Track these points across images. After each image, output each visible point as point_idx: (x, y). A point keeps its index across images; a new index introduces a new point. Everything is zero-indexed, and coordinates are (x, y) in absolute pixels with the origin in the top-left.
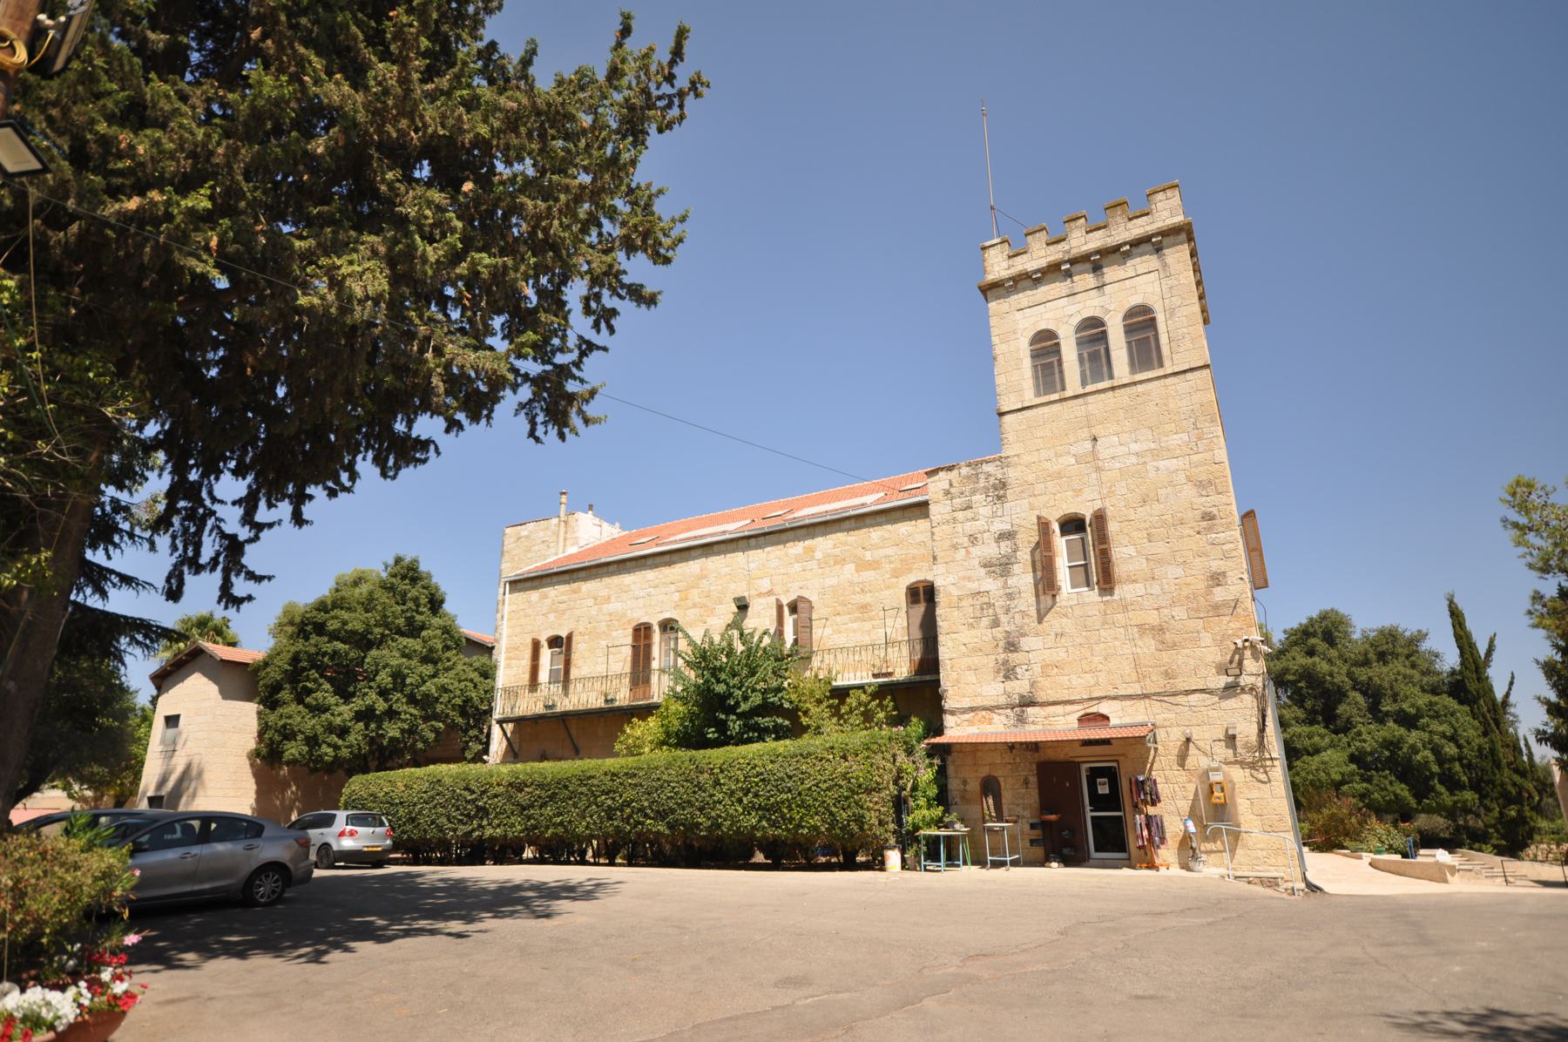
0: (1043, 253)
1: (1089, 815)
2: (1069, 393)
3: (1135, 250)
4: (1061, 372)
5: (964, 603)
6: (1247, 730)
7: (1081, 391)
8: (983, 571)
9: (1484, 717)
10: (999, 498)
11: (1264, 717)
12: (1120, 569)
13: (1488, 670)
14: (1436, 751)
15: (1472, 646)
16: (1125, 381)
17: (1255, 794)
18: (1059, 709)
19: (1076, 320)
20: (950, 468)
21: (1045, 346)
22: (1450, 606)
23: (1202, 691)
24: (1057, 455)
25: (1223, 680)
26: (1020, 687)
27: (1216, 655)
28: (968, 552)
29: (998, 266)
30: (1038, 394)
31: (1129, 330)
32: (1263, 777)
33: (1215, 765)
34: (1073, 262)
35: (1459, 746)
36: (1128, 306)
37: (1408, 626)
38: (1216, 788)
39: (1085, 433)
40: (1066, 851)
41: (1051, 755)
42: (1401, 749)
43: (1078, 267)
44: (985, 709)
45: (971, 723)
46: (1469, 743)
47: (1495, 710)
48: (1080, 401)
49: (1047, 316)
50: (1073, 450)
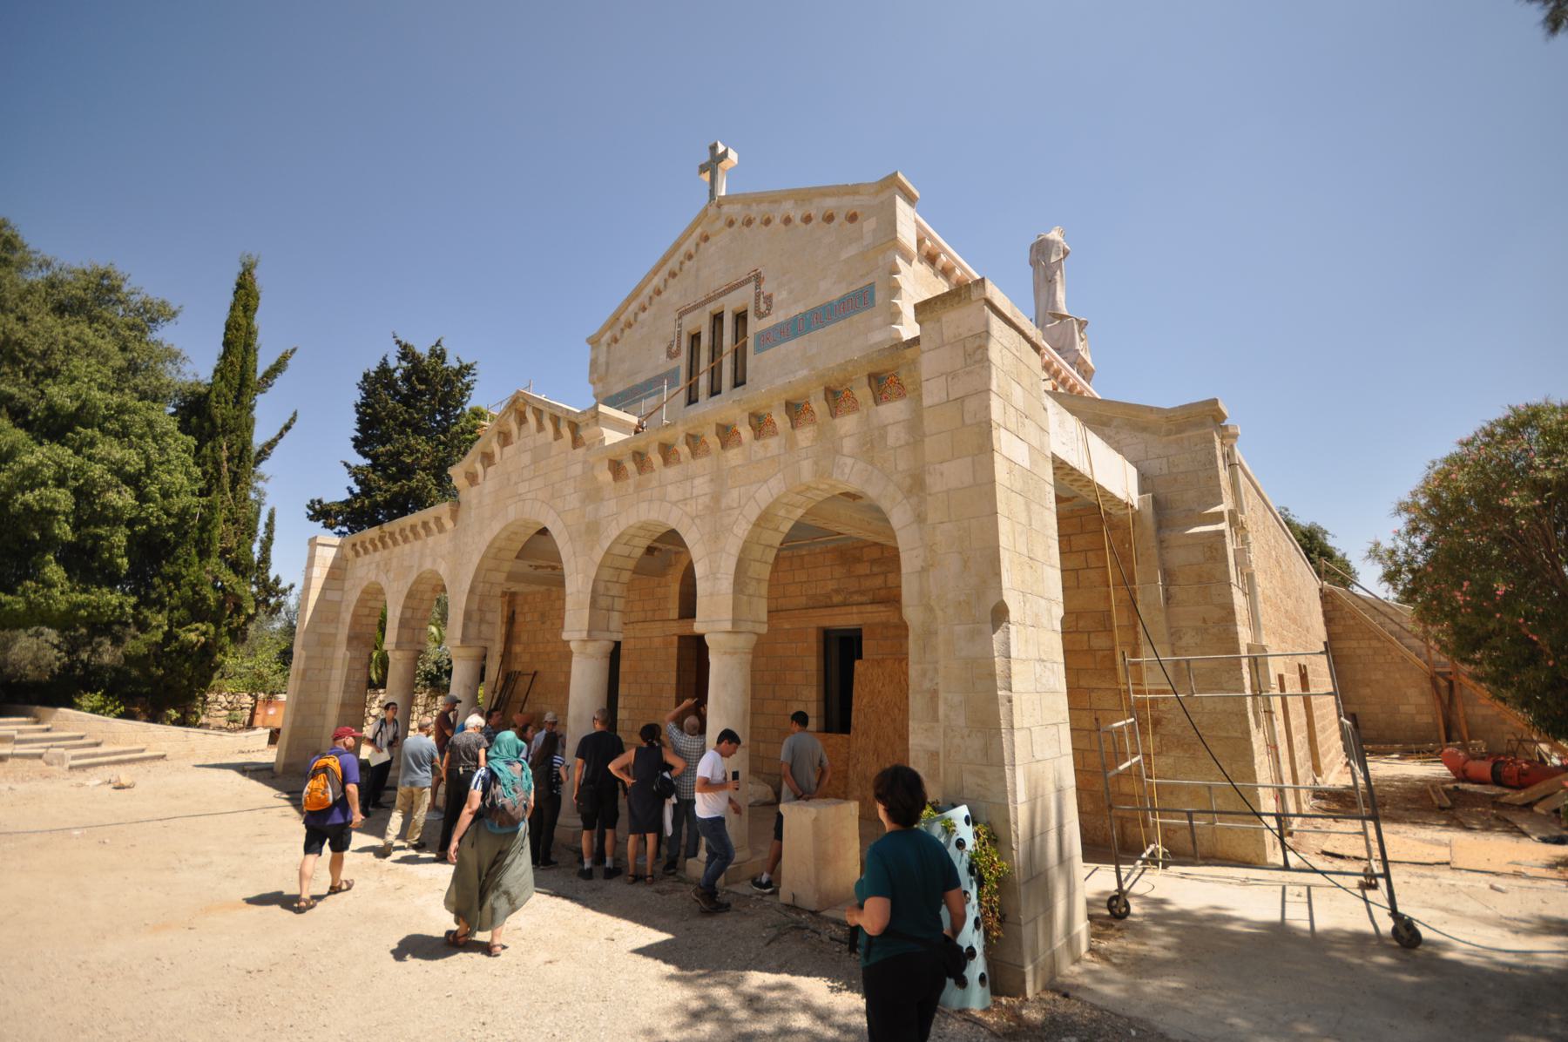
9: (217, 464)
13: (259, 397)
14: (83, 494)
15: (249, 349)
22: (240, 286)
35: (142, 497)
46: (166, 495)
47: (241, 459)
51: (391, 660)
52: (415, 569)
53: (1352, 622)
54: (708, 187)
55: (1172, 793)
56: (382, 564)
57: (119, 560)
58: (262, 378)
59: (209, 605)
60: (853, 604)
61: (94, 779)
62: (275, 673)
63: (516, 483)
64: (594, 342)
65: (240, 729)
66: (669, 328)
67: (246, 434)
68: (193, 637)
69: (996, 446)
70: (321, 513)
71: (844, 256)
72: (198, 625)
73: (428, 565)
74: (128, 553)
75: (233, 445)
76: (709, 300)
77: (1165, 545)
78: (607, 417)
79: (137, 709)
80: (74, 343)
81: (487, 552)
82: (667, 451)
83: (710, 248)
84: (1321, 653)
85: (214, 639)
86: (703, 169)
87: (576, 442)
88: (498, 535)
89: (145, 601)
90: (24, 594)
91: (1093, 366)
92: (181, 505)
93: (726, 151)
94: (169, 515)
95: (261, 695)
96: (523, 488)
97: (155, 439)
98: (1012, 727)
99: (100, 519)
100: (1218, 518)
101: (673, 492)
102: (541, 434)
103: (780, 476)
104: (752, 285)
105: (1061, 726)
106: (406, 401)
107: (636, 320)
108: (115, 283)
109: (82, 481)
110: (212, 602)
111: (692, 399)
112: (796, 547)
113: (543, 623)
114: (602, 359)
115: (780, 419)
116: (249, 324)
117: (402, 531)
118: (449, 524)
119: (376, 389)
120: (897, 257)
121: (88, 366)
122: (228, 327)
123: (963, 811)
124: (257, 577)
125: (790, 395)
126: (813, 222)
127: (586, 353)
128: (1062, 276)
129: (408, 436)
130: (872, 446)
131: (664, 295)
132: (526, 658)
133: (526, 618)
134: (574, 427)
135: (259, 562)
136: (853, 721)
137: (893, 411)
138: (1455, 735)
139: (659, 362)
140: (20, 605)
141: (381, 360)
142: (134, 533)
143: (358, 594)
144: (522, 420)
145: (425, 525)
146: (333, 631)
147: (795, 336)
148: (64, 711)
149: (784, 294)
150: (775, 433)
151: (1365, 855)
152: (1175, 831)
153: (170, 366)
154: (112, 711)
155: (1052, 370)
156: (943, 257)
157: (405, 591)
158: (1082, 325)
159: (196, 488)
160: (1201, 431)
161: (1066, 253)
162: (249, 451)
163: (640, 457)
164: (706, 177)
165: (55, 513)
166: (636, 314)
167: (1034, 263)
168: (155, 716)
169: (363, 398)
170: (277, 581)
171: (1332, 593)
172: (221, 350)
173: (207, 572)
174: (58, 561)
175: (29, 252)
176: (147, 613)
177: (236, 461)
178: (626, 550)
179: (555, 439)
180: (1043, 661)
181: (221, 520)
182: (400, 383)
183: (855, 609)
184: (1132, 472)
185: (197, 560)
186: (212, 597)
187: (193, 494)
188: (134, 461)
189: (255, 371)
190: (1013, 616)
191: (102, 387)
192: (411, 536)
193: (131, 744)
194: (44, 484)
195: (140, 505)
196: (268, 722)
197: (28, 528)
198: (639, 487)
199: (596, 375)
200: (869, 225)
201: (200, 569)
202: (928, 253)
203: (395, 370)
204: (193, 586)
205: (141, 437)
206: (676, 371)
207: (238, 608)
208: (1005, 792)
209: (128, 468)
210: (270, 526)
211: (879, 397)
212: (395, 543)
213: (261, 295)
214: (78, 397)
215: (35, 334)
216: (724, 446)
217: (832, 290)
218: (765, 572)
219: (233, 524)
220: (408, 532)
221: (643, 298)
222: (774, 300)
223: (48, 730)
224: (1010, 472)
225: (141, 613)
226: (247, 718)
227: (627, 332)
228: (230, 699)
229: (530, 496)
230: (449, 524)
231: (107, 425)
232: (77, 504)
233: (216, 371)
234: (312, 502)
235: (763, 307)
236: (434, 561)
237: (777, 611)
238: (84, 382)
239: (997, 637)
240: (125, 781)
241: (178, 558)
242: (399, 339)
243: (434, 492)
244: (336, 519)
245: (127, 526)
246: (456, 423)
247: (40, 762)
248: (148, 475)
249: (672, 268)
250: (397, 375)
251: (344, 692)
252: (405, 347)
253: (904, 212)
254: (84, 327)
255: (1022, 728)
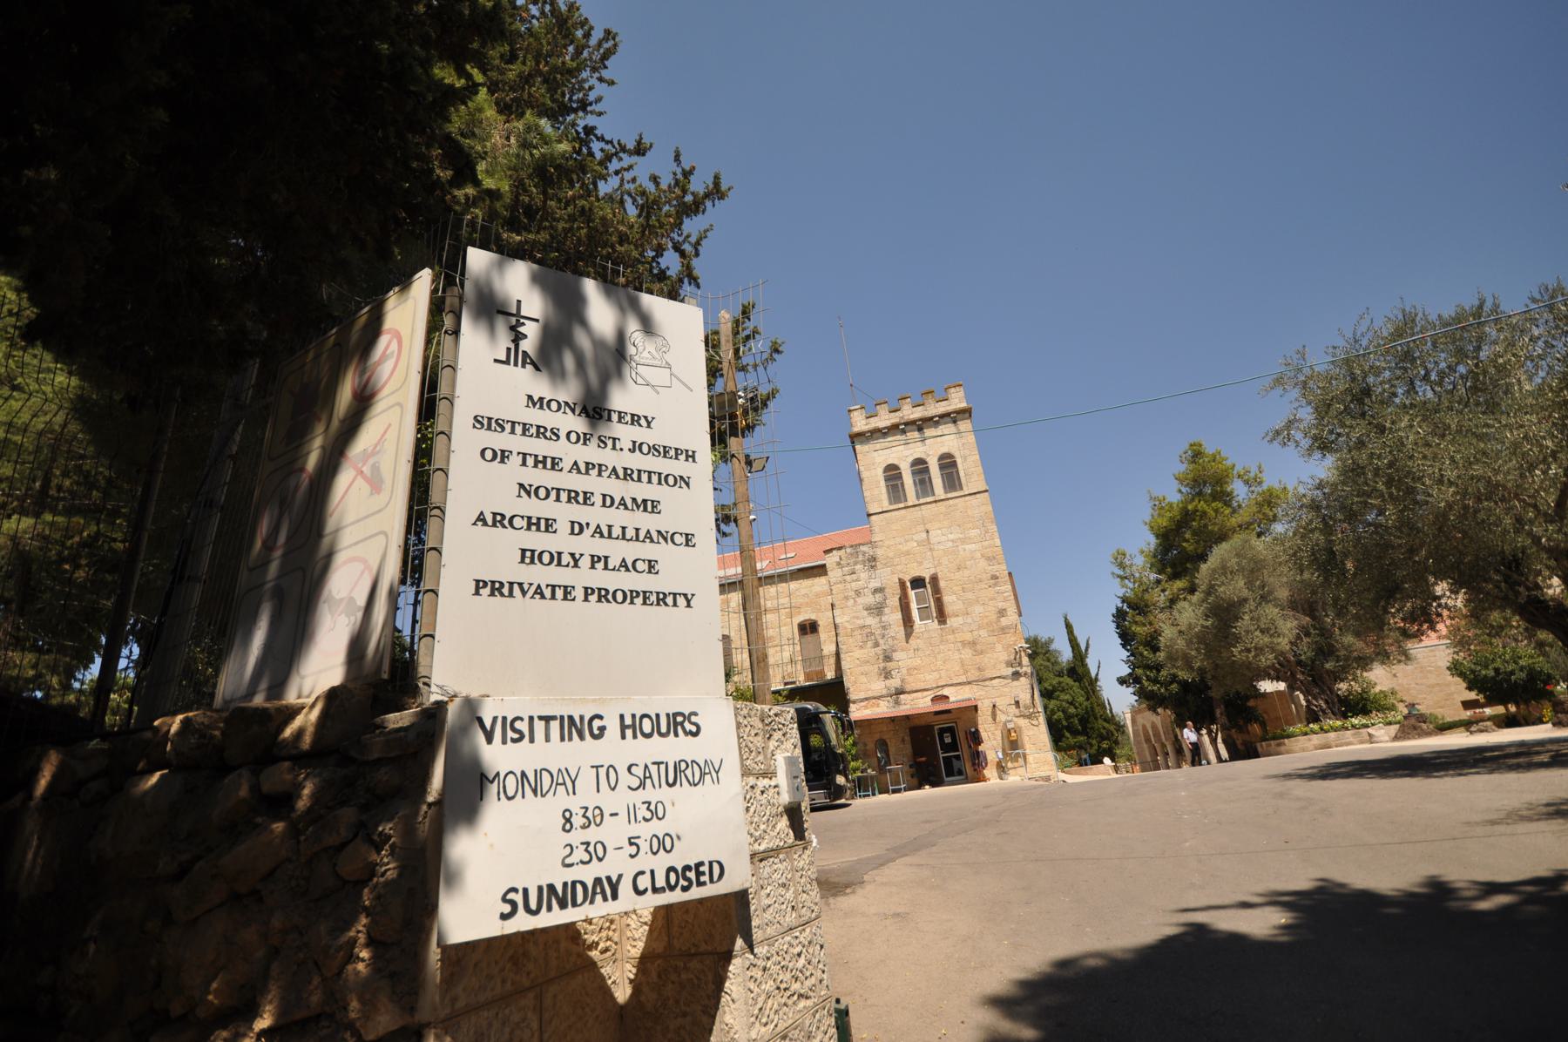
0: (887, 417)
1: (941, 756)
2: (910, 504)
3: (941, 421)
4: (904, 490)
5: (855, 633)
6: (1025, 697)
7: (917, 503)
8: (866, 613)
10: (872, 567)
11: (1033, 689)
12: (948, 609)
15: (1078, 645)
16: (943, 497)
17: (1031, 733)
18: (919, 694)
19: (911, 459)
20: (840, 548)
21: (892, 473)
23: (999, 677)
24: (906, 541)
25: (1010, 671)
26: (895, 683)
27: (1004, 656)
28: (855, 601)
29: (860, 423)
30: (891, 504)
31: (942, 467)
32: (1034, 722)
33: (1010, 718)
34: (906, 424)
35: (1076, 708)
36: (940, 453)
38: (1012, 731)
39: (921, 528)
40: (931, 778)
41: (917, 722)
43: (909, 427)
44: (875, 698)
45: (866, 707)
48: (917, 508)
49: (894, 455)
50: (915, 537)
70: (1122, 681)
89: (1089, 737)
186: (1104, 732)
188: (1070, 699)
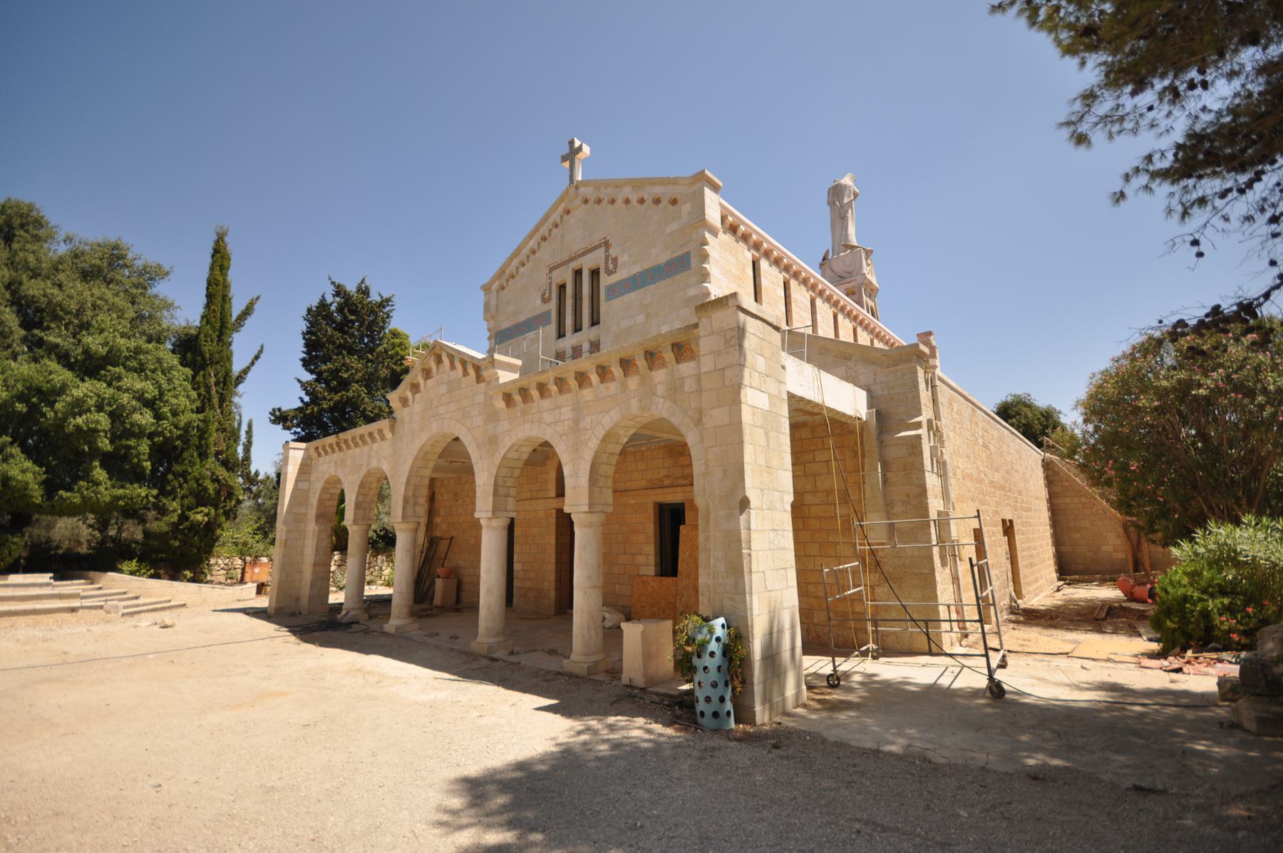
9: (208, 388)
13: (235, 336)
15: (225, 299)
35: (158, 417)
37: (142, 251)
42: (51, 404)
51: (350, 532)
52: (365, 467)
53: (1067, 484)
54: (568, 173)
55: (886, 611)
56: (339, 463)
57: (145, 464)
58: (236, 321)
59: (209, 494)
60: (678, 486)
61: (145, 621)
62: (258, 542)
63: (437, 407)
64: (486, 288)
65: (235, 583)
66: (542, 279)
67: (227, 364)
68: (199, 517)
69: (743, 399)
70: (280, 418)
71: (668, 231)
72: (203, 508)
73: (374, 464)
74: (150, 458)
75: (218, 373)
76: (572, 259)
77: (884, 444)
78: (500, 362)
79: (162, 572)
80: (99, 302)
81: (417, 455)
82: (542, 388)
83: (571, 220)
84: (975, 517)
85: (215, 519)
86: (564, 159)
87: (479, 379)
88: (426, 442)
89: (163, 492)
90: (79, 491)
91: (877, 286)
92: (185, 421)
93: (581, 145)
94: (176, 427)
95: (248, 559)
96: (442, 410)
97: (163, 372)
98: (751, 571)
99: (129, 434)
100: (919, 425)
101: (548, 417)
102: (454, 372)
103: (617, 408)
104: (602, 249)
105: (788, 570)
106: (342, 327)
107: (517, 272)
108: (123, 252)
109: (115, 407)
110: (211, 491)
111: (561, 334)
112: (637, 445)
113: (456, 501)
114: (493, 302)
115: (617, 371)
116: (224, 280)
117: (354, 438)
118: (388, 435)
119: (316, 321)
120: (706, 233)
121: (111, 320)
122: (209, 283)
123: (722, 620)
124: (242, 472)
125: (623, 355)
126: (646, 204)
127: (480, 297)
128: (852, 214)
129: (344, 357)
130: (675, 391)
131: (538, 255)
132: (444, 527)
133: (443, 497)
134: (477, 369)
135: (243, 461)
136: (680, 568)
137: (686, 368)
138: (1141, 567)
139: (534, 305)
140: (77, 500)
141: (320, 297)
142: (154, 443)
143: (322, 483)
144: (439, 361)
145: (371, 434)
146: (304, 511)
147: (635, 289)
148: (112, 575)
149: (626, 258)
150: (614, 379)
151: (999, 647)
152: (888, 636)
153: (165, 313)
154: (144, 573)
155: (832, 301)
156: (742, 228)
157: (358, 483)
158: (869, 253)
159: (194, 407)
160: (909, 365)
161: (856, 195)
162: (230, 377)
163: (524, 392)
164: (567, 164)
165: (95, 431)
166: (517, 268)
167: (831, 204)
168: (174, 576)
169: (308, 327)
170: (257, 474)
171: (1052, 462)
172: (205, 300)
173: (207, 469)
174: (102, 466)
175: (52, 228)
176: (165, 501)
177: (222, 385)
178: (516, 455)
179: (464, 376)
180: (776, 530)
181: (214, 430)
182: (335, 314)
183: (679, 489)
184: (862, 395)
185: (198, 460)
186: (211, 487)
187: (192, 411)
188: (150, 390)
189: (231, 316)
190: (752, 505)
191: (123, 335)
192: (360, 442)
193: (161, 597)
194: (89, 410)
195: (157, 423)
196: (255, 578)
197: (79, 443)
198: (524, 413)
199: (488, 315)
200: (686, 208)
201: (201, 467)
202: (731, 225)
203: (331, 304)
204: (197, 480)
205: (153, 371)
206: (548, 313)
207: (230, 495)
208: (746, 609)
209: (146, 395)
210: (249, 433)
211: (679, 360)
212: (348, 447)
213: (232, 257)
214: (106, 344)
215: (71, 297)
216: (581, 386)
217: (661, 256)
218: (610, 471)
219: (222, 432)
220: (358, 440)
221: (523, 256)
222: (619, 262)
223: (100, 588)
224: (754, 414)
225: (160, 501)
226: (239, 576)
227: (511, 281)
228: (227, 561)
229: (446, 416)
230: (388, 435)
231: (128, 363)
232: (112, 424)
233: (202, 317)
234: (274, 410)
235: (611, 267)
236: (379, 461)
237: (625, 491)
238: (110, 332)
239: (743, 518)
240: (168, 622)
241: (185, 459)
242: (333, 280)
243: (367, 400)
244: (292, 422)
245: (148, 438)
246: (380, 344)
247: (101, 612)
248: (161, 399)
249: (544, 233)
250: (333, 308)
251: (316, 555)
252: (338, 286)
253: (710, 196)
254: (103, 289)
255: (758, 572)
